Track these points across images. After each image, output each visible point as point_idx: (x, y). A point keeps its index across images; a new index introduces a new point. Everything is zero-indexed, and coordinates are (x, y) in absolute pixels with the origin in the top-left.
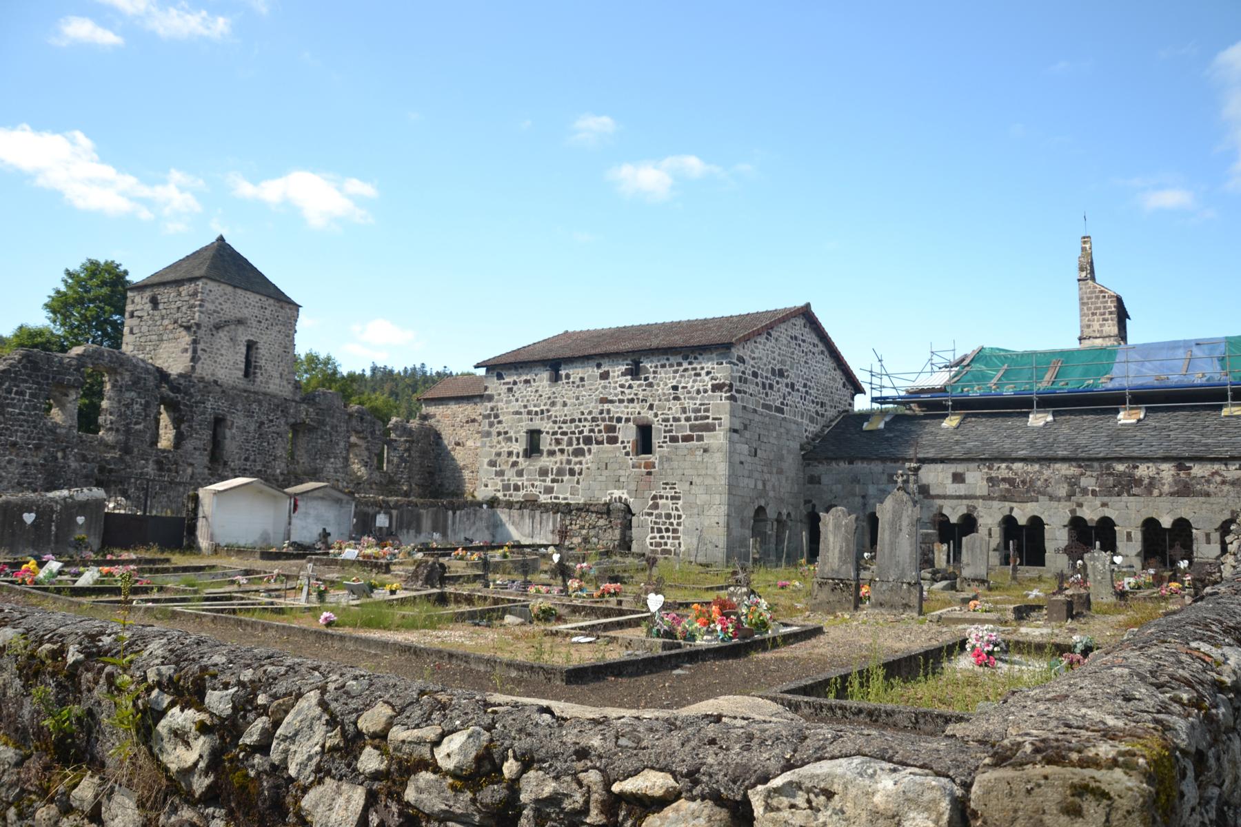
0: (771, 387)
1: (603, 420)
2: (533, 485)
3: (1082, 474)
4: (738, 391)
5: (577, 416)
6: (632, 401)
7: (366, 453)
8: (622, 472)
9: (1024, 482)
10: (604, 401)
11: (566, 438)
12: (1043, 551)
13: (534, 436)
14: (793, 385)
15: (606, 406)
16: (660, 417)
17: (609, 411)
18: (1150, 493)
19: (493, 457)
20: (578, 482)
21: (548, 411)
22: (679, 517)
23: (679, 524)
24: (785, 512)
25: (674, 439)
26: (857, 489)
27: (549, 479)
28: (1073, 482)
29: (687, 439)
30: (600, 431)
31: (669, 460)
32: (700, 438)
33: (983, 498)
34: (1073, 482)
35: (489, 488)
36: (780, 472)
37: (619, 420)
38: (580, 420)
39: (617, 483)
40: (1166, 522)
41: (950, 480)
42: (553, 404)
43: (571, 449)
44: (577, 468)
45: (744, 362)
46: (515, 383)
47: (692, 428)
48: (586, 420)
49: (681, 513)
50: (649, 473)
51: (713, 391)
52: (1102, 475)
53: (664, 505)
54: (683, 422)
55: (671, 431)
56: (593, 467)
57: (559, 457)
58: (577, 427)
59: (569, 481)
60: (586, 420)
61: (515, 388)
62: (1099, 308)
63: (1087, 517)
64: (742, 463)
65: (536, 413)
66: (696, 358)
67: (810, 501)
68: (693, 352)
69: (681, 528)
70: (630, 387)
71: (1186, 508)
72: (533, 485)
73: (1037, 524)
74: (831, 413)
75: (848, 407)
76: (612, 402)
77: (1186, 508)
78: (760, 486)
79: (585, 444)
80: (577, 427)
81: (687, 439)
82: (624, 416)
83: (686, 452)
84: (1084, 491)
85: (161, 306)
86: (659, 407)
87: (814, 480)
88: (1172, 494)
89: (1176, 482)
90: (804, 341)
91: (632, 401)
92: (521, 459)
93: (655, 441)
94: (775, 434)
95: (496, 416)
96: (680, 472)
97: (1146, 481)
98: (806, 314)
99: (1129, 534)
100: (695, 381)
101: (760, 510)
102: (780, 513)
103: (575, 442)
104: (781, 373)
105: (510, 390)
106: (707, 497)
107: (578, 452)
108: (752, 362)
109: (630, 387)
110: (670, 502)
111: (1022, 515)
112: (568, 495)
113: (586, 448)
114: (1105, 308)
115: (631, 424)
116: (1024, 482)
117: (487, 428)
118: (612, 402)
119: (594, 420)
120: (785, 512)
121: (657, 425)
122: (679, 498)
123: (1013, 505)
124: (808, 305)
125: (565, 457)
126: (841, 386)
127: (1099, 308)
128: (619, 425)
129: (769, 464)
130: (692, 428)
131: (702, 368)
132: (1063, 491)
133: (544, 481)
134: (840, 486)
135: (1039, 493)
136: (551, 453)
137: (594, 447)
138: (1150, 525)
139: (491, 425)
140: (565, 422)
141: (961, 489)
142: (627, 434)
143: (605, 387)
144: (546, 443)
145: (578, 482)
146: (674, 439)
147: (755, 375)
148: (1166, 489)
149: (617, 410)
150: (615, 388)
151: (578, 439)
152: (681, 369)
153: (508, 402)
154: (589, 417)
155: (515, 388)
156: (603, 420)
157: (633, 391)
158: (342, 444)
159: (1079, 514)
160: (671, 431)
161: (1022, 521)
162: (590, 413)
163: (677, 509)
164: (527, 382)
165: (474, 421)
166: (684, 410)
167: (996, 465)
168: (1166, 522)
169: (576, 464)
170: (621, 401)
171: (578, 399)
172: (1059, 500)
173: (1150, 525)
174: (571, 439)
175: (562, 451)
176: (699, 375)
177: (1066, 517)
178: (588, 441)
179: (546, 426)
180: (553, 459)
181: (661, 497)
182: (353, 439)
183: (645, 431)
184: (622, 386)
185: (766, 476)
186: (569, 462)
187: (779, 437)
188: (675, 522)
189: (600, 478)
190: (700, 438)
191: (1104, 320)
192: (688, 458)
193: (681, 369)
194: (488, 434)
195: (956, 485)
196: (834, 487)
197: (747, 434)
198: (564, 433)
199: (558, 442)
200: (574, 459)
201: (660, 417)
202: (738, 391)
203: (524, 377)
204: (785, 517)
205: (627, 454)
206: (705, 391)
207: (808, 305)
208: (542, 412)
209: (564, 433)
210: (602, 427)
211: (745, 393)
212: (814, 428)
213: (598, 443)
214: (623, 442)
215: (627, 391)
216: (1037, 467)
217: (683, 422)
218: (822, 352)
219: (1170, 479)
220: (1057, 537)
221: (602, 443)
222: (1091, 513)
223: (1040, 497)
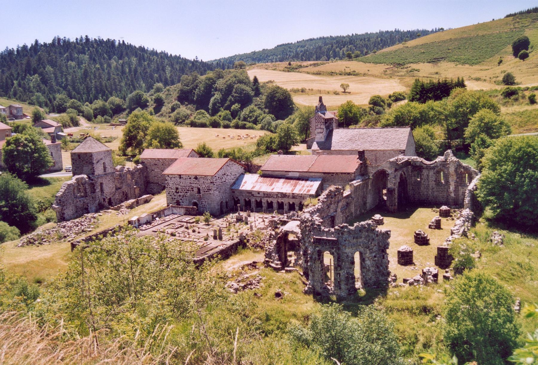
34: (277, 195)
39: (195, 199)
40: (291, 203)
73: (272, 202)
142: (196, 190)
144: (180, 190)
149: (193, 185)
168: (291, 203)
179: (179, 187)
183: (199, 189)
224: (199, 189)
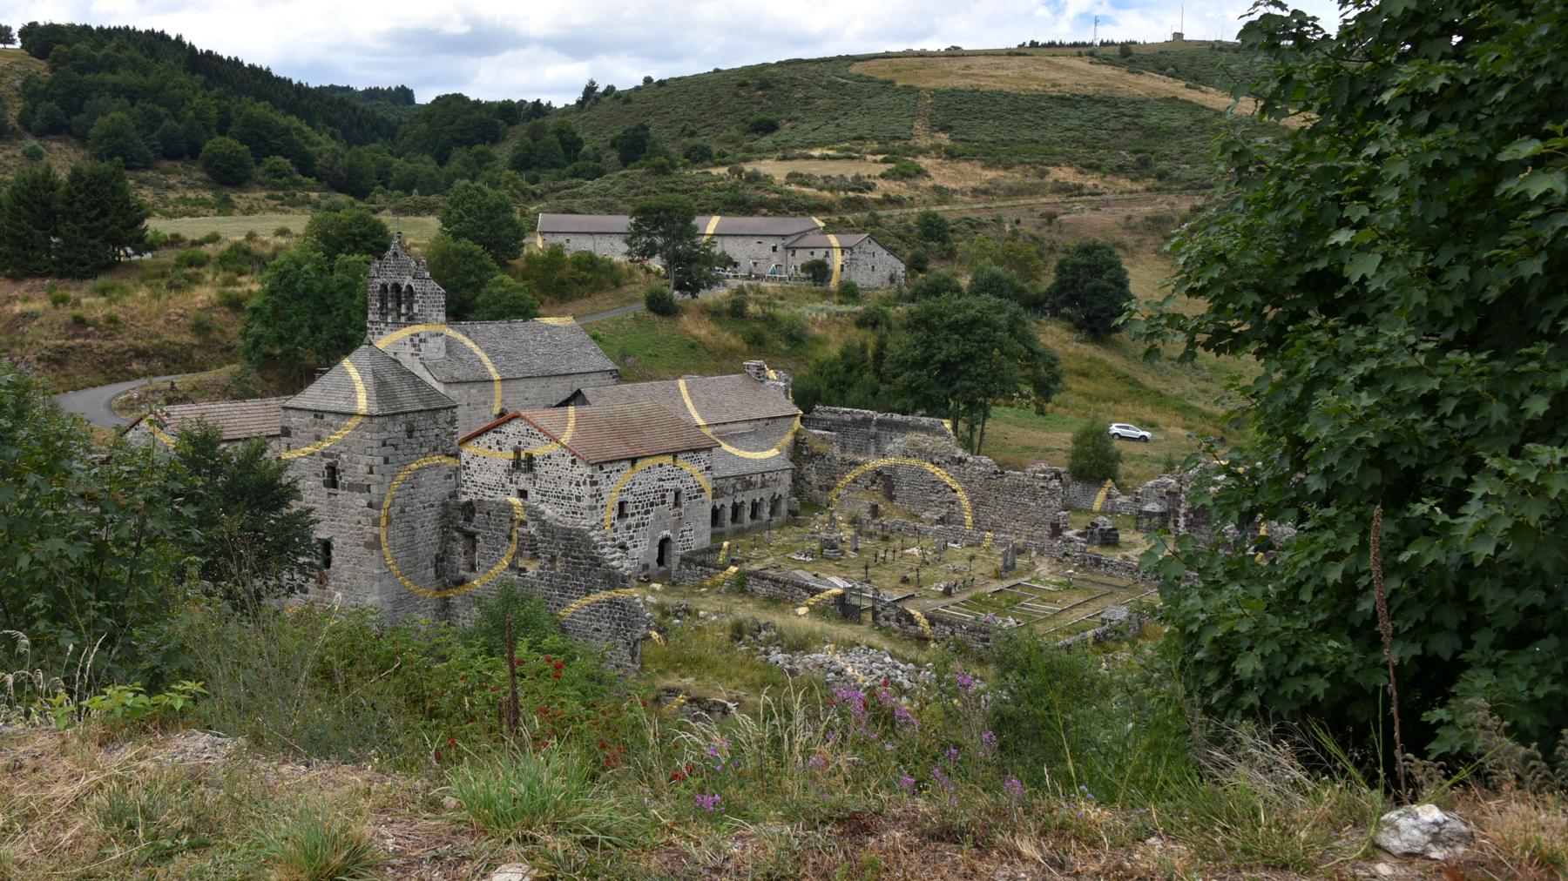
34: (734, 486)
85: (417, 434)
107: (647, 512)
121: (684, 491)
142: (670, 498)
144: (629, 509)
149: (667, 485)
178: (652, 504)
179: (630, 498)
183: (678, 494)
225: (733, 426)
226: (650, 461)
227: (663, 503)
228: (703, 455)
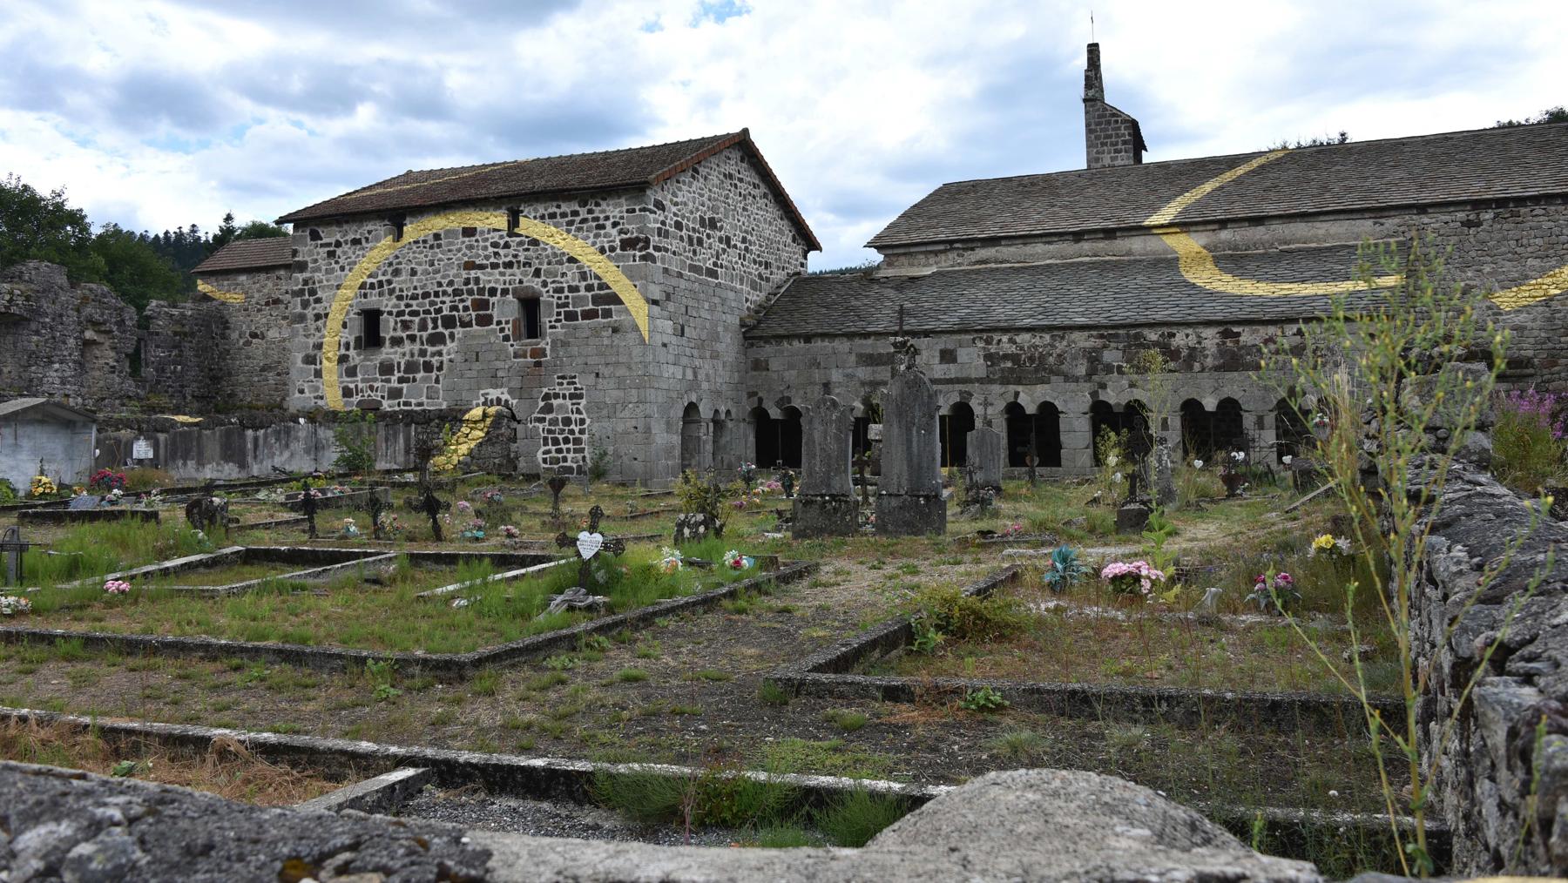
0: (700, 242)
1: (470, 292)
2: (371, 388)
3: (1105, 347)
4: (657, 249)
5: (432, 288)
6: (509, 265)
7: (112, 354)
8: (499, 364)
9: (1032, 359)
10: (470, 266)
11: (417, 319)
12: (1058, 446)
13: (371, 318)
14: (728, 240)
15: (473, 273)
16: (550, 286)
17: (477, 280)
18: (1190, 368)
19: (311, 352)
20: (437, 381)
21: (389, 282)
22: (582, 422)
23: (582, 432)
24: (723, 409)
25: (571, 316)
26: (817, 375)
27: (394, 378)
28: (1093, 358)
29: (588, 315)
30: (466, 309)
31: (565, 344)
32: (607, 314)
33: (980, 381)
34: (1093, 358)
35: (307, 394)
36: (715, 356)
37: (493, 292)
38: (436, 294)
40: (1210, 404)
41: (937, 360)
42: (397, 273)
43: (425, 334)
44: (435, 360)
45: (663, 209)
46: (338, 244)
47: (596, 300)
48: (445, 293)
49: (584, 416)
50: (538, 364)
51: (623, 249)
52: (1130, 346)
53: (560, 406)
54: (582, 292)
55: (566, 305)
56: (459, 358)
57: (407, 346)
58: (432, 303)
59: (424, 380)
60: (445, 293)
61: (339, 251)
62: (1110, 136)
63: (1112, 402)
64: (665, 345)
65: (372, 285)
66: (597, 205)
67: (755, 394)
68: (593, 196)
69: (585, 437)
70: (507, 246)
71: (1235, 386)
72: (371, 388)
73: (1049, 412)
74: (778, 276)
75: (800, 269)
76: (482, 267)
77: (1235, 386)
78: (690, 375)
79: (446, 326)
80: (432, 303)
81: (588, 315)
82: (500, 287)
83: (588, 333)
84: (1109, 369)
86: (548, 273)
87: (759, 366)
88: (1217, 368)
89: (1222, 351)
90: (741, 180)
91: (509, 265)
92: (352, 352)
93: (546, 321)
94: (706, 306)
95: (313, 292)
96: (580, 360)
97: (1185, 353)
98: (742, 145)
99: (1165, 421)
100: (597, 236)
101: (691, 409)
102: (717, 411)
103: (430, 325)
104: (713, 224)
105: (331, 254)
106: (621, 393)
107: (437, 339)
108: (674, 209)
109: (507, 246)
110: (568, 402)
111: (1029, 400)
112: (424, 399)
113: (447, 332)
114: (1117, 136)
115: (510, 297)
116: (1032, 359)
117: (299, 310)
118: (482, 267)
119: (457, 292)
120: (723, 409)
122: (580, 397)
123: (1020, 388)
124: (745, 131)
125: (417, 347)
126: (789, 241)
127: (1110, 136)
128: (492, 300)
129: (701, 345)
130: (596, 300)
131: (607, 218)
132: (1082, 370)
133: (389, 381)
134: (794, 372)
135: (1052, 372)
136: (397, 342)
137: (459, 331)
138: (1191, 409)
139: (305, 305)
140: (414, 297)
141: (952, 371)
142: (506, 311)
143: (470, 247)
145: (437, 381)
146: (571, 316)
147: (678, 226)
148: (1209, 362)
149: (489, 278)
150: (485, 248)
151: (435, 321)
152: (578, 219)
153: (329, 271)
154: (450, 290)
155: (339, 251)
156: (470, 292)
157: (511, 251)
158: (71, 342)
159: (1101, 398)
160: (566, 305)
161: (1031, 409)
162: (451, 283)
163: (579, 411)
164: (356, 242)
165: (277, 302)
166: (583, 276)
167: (996, 337)
168: (1210, 404)
169: (433, 355)
170: (495, 266)
171: (432, 264)
172: (1077, 380)
173: (1191, 409)
174: (423, 322)
175: (412, 338)
176: (603, 227)
177: (1085, 401)
178: (449, 322)
179: (388, 304)
180: (400, 350)
181: (556, 396)
182: (89, 334)
183: (530, 305)
184: (495, 245)
185: (697, 362)
186: (423, 353)
187: (712, 310)
188: (577, 430)
189: (468, 374)
190: (607, 314)
191: (1116, 151)
192: (592, 341)
193: (578, 219)
194: (301, 318)
195: (945, 366)
196: (786, 374)
197: (671, 306)
198: (414, 313)
199: (406, 326)
200: (430, 349)
201: (550, 286)
202: (657, 249)
203: (351, 237)
204: (723, 416)
205: (506, 338)
206: (612, 249)
207: (745, 131)
208: (381, 284)
209: (414, 313)
210: (469, 303)
211: (667, 250)
212: (757, 297)
213: (464, 325)
214: (499, 323)
215: (502, 252)
216: (1047, 337)
217: (582, 292)
218: (765, 196)
219: (1214, 349)
220: (1075, 431)
221: (469, 324)
222: (1115, 396)
223: (1053, 378)
224: (530, 305)
225: (1300, 229)
226: (438, 223)
227: (485, 321)
228: (614, 209)
